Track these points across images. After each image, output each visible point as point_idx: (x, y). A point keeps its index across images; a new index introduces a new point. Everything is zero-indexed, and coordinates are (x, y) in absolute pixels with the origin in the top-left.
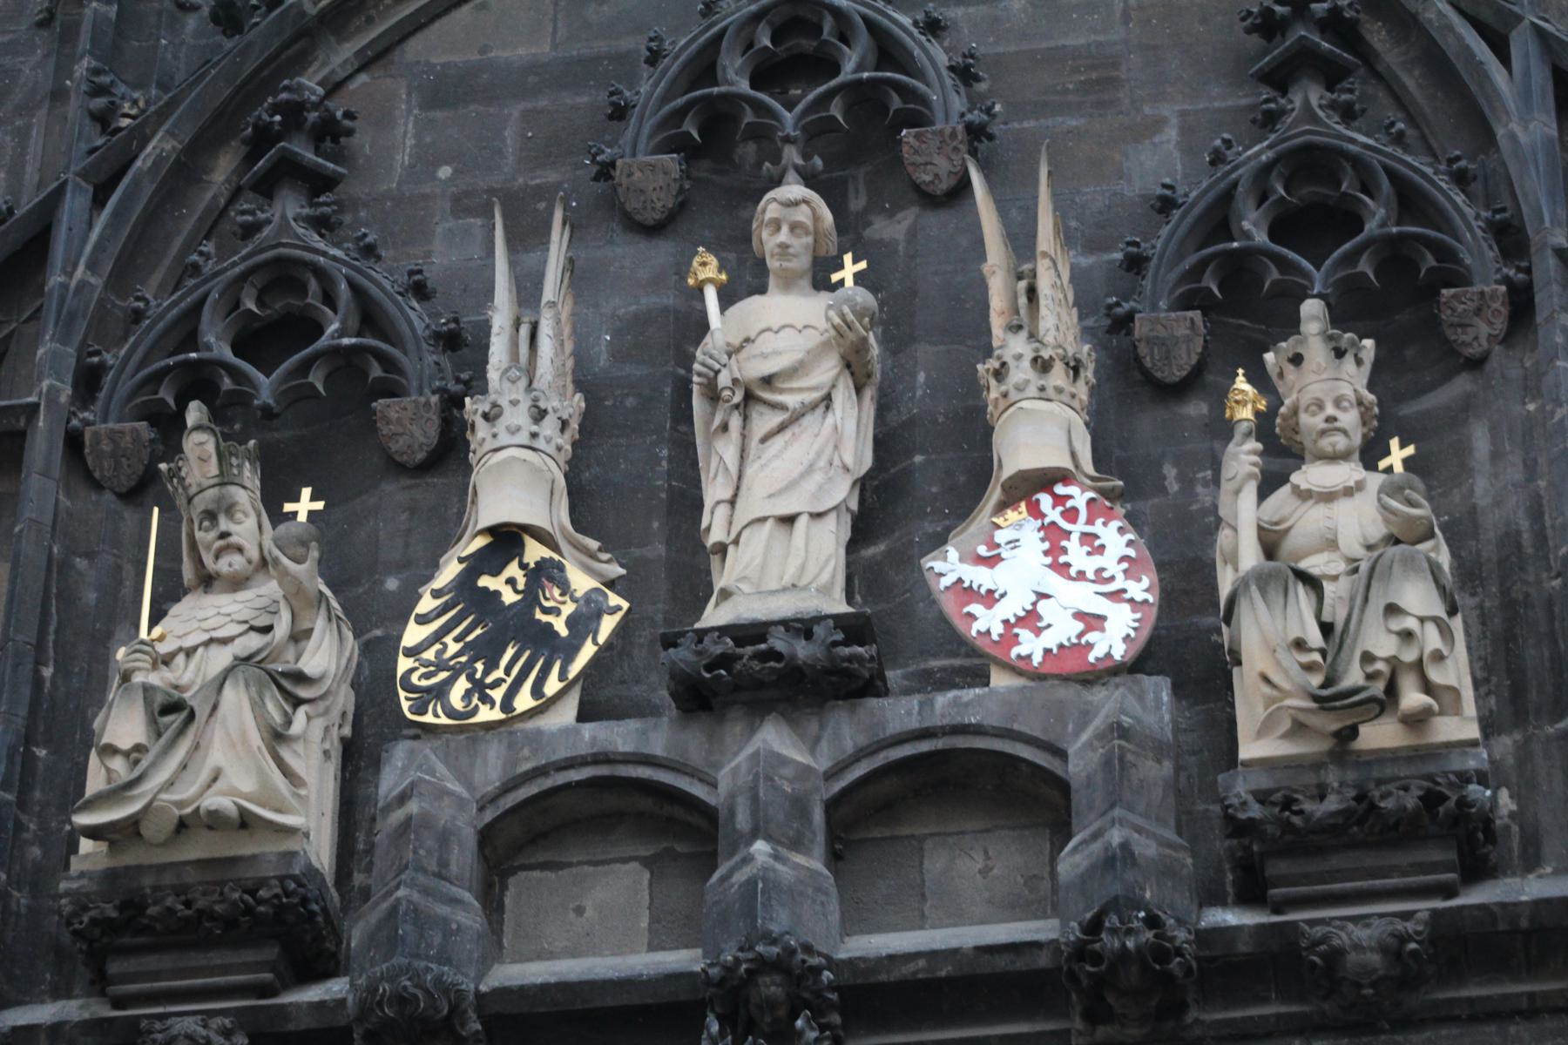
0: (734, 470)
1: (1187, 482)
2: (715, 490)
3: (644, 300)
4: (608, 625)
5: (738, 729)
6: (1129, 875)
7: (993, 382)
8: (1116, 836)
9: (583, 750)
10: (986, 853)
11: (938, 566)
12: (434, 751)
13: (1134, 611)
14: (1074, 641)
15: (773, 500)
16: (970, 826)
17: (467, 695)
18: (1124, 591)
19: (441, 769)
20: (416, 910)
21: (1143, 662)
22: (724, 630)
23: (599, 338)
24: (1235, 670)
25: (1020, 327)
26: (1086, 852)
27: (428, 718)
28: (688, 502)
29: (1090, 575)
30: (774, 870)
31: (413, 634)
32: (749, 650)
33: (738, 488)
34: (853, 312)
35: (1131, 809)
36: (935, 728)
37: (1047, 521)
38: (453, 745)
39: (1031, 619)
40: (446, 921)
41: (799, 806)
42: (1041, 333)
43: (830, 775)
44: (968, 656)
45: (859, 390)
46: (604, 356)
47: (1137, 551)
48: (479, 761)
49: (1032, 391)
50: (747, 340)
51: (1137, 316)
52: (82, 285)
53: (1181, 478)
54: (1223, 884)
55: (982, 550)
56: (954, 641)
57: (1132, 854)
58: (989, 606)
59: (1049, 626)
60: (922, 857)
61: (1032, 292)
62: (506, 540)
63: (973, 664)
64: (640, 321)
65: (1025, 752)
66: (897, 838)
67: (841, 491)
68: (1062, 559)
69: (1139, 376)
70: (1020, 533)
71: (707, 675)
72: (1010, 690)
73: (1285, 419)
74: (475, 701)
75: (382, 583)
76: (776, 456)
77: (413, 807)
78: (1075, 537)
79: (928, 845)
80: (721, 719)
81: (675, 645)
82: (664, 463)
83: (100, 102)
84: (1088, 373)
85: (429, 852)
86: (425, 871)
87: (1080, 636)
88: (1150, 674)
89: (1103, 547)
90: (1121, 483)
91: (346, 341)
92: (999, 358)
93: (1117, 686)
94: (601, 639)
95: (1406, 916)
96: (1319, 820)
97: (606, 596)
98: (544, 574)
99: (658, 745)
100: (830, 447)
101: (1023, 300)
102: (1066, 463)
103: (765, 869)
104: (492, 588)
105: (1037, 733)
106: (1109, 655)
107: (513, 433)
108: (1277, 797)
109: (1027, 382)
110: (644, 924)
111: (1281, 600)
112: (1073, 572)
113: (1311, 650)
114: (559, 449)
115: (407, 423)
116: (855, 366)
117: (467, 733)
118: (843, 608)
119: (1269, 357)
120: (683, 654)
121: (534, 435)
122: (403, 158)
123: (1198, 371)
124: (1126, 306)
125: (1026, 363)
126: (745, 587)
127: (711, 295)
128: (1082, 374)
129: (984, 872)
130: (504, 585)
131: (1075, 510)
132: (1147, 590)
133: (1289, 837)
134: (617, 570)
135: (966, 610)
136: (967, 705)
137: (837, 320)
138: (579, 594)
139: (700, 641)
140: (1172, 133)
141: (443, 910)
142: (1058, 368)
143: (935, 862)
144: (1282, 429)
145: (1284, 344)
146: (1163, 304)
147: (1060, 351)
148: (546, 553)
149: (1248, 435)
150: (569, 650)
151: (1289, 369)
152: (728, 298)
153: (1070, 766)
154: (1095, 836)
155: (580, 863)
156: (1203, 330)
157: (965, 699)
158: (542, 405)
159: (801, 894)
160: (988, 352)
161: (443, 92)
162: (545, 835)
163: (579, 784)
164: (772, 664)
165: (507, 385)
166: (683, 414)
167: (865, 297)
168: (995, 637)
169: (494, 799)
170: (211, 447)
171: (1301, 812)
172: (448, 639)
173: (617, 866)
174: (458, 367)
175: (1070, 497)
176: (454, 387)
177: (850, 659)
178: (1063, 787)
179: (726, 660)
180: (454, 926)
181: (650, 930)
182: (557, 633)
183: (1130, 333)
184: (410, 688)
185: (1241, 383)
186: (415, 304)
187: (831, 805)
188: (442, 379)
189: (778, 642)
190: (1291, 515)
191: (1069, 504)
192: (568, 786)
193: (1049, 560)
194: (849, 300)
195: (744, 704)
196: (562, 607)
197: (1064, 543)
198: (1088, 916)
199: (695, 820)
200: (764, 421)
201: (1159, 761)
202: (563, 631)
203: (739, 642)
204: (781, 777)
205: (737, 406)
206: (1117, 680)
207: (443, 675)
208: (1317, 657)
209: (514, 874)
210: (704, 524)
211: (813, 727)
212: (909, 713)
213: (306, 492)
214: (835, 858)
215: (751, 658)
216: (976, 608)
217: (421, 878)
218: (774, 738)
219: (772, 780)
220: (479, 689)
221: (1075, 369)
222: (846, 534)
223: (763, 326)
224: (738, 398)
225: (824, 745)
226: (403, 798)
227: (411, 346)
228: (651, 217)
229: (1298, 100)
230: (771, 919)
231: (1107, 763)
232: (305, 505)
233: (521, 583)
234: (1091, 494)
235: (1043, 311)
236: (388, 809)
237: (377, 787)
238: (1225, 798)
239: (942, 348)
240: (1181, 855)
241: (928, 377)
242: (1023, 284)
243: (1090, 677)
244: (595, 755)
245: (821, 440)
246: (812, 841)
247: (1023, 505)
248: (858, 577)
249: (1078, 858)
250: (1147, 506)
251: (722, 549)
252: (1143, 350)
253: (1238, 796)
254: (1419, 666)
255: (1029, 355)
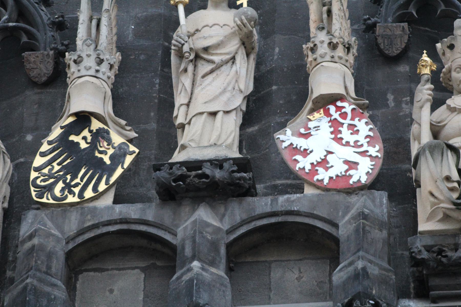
0: (189, 90)
1: (398, 103)
2: (180, 99)
3: (150, 10)
4: (129, 160)
5: (187, 209)
6: (366, 283)
7: (310, 53)
8: (360, 264)
9: (116, 216)
10: (300, 270)
11: (282, 137)
12: (46, 215)
13: (371, 161)
14: (343, 173)
15: (207, 105)
16: (293, 258)
17: (63, 190)
18: (367, 151)
19: (49, 224)
20: (35, 289)
21: (375, 184)
22: (182, 164)
23: (129, 27)
24: (418, 190)
25: (323, 28)
26: (346, 271)
27: (44, 200)
28: (167, 104)
29: (352, 144)
30: (202, 275)
31: (38, 161)
32: (194, 173)
33: (191, 99)
34: (246, 19)
35: (367, 252)
36: (278, 211)
37: (333, 118)
38: (55, 213)
39: (323, 163)
40: (49, 294)
41: (214, 245)
42: (333, 31)
43: (229, 232)
44: (294, 179)
45: (248, 55)
46: (131, 35)
47: (374, 133)
48: (67, 221)
49: (328, 58)
50: (197, 30)
51: (378, 24)
53: (395, 100)
54: (409, 288)
55: (302, 131)
56: (288, 172)
57: (368, 273)
58: (305, 157)
59: (332, 166)
60: (270, 271)
61: (329, 12)
62: (83, 119)
63: (296, 182)
64: (148, 20)
65: (319, 224)
66: (259, 262)
67: (238, 101)
68: (339, 136)
69: (378, 53)
70: (320, 123)
71: (174, 184)
72: (313, 195)
73: (445, 74)
74: (66, 193)
75: (25, 137)
76: (209, 84)
77: (36, 241)
78: (345, 126)
79: (273, 265)
80: (180, 205)
81: (160, 170)
82: (157, 86)
84: (354, 50)
85: (42, 262)
86: (39, 270)
87: (346, 171)
88: (378, 190)
89: (358, 131)
90: (367, 102)
91: (11, 24)
92: (313, 42)
93: (363, 195)
94: (126, 166)
96: (455, 260)
97: (128, 146)
99: (150, 216)
100: (234, 81)
101: (325, 16)
102: (343, 92)
103: (197, 274)
104: (75, 141)
105: (325, 216)
106: (359, 181)
107: (88, 70)
108: (435, 249)
109: (326, 53)
110: (141, 298)
111: (440, 158)
112: (344, 142)
113: (454, 182)
114: (109, 78)
115: (38, 63)
116: (246, 44)
117: (61, 207)
118: (237, 155)
119: (439, 45)
120: (163, 174)
121: (97, 71)
123: (405, 52)
124: (373, 20)
125: (326, 45)
126: (193, 144)
127: (181, 9)
128: (351, 51)
129: (299, 279)
130: (81, 140)
131: (346, 113)
132: (377, 152)
133: (440, 268)
134: (133, 135)
135: (294, 158)
136: (293, 201)
137: (239, 22)
138: (116, 145)
139: (171, 168)
141: (48, 289)
142: (340, 47)
143: (276, 274)
144: (443, 79)
145: (446, 40)
146: (390, 19)
147: (341, 40)
148: (101, 126)
149: (427, 81)
150: (111, 170)
151: (448, 51)
152: (189, 11)
153: (340, 232)
154: (350, 264)
155: (112, 269)
156: (408, 32)
157: (292, 199)
158: (102, 57)
159: (214, 286)
160: (308, 39)
162: (97, 256)
163: (113, 232)
164: (204, 180)
165: (85, 47)
166: (168, 64)
167: (252, 12)
168: (307, 171)
169: (73, 238)
171: (446, 256)
172: (55, 164)
173: (130, 271)
174: (63, 38)
175: (344, 107)
176: (60, 47)
177: (240, 179)
178: (336, 241)
179: (182, 178)
180: (53, 297)
181: (143, 301)
182: (105, 163)
183: (374, 32)
184: (36, 186)
185: (425, 57)
186: (44, 8)
187: (229, 246)
188: (55, 43)
189: (207, 170)
190: (446, 119)
191: (343, 110)
192: (108, 233)
193: (333, 136)
194: (244, 13)
195: (190, 198)
196: (108, 151)
197: (340, 129)
198: (346, 301)
199: (166, 250)
200: (204, 68)
201: (381, 230)
202: (108, 162)
203: (189, 169)
204: (206, 232)
205: (191, 61)
206: (363, 192)
207: (52, 180)
208: (456, 185)
209: (82, 273)
210: (175, 115)
211: (222, 209)
212: (266, 204)
214: (230, 270)
215: (194, 177)
217: (38, 274)
218: (204, 214)
219: (202, 233)
220: (68, 187)
221: (348, 48)
222: (240, 121)
223: (205, 24)
224: (192, 57)
225: (227, 218)
226: (31, 237)
227: (41, 28)
230: (200, 298)
231: (357, 231)
233: (89, 139)
234: (353, 106)
235: (334, 21)
236: (24, 242)
237: (19, 231)
238: (411, 249)
239: (287, 37)
240: (390, 274)
241: (280, 50)
242: (325, 8)
243: (351, 191)
244: (121, 219)
245: (229, 77)
246: (220, 262)
247: (322, 111)
248: (245, 141)
249: (342, 274)
250: (379, 113)
251: (182, 126)
252: (380, 40)
253: (417, 247)
255: (327, 41)
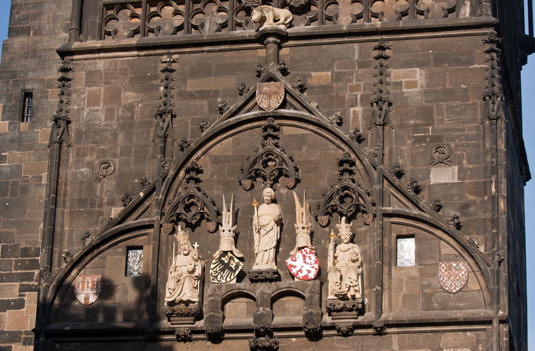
2: (256, 242)
4: (240, 268)
9: (237, 288)
11: (287, 261)
27: (214, 281)
31: (212, 266)
32: (259, 275)
39: (300, 271)
40: (217, 316)
49: (302, 232)
52: (161, 199)
55: (294, 259)
62: (225, 253)
70: (299, 255)
83: (163, 163)
95: (350, 322)
98: (231, 258)
122: (209, 173)
130: (225, 260)
134: (241, 255)
140: (326, 178)
141: (217, 314)
150: (234, 271)
161: (216, 160)
170: (182, 235)
179: (256, 277)
208: (339, 284)
213: (196, 243)
216: (292, 268)
220: (222, 276)
228: (247, 189)
229: (344, 177)
231: (310, 296)
232: (196, 245)
251: (257, 254)
254: (353, 286)
